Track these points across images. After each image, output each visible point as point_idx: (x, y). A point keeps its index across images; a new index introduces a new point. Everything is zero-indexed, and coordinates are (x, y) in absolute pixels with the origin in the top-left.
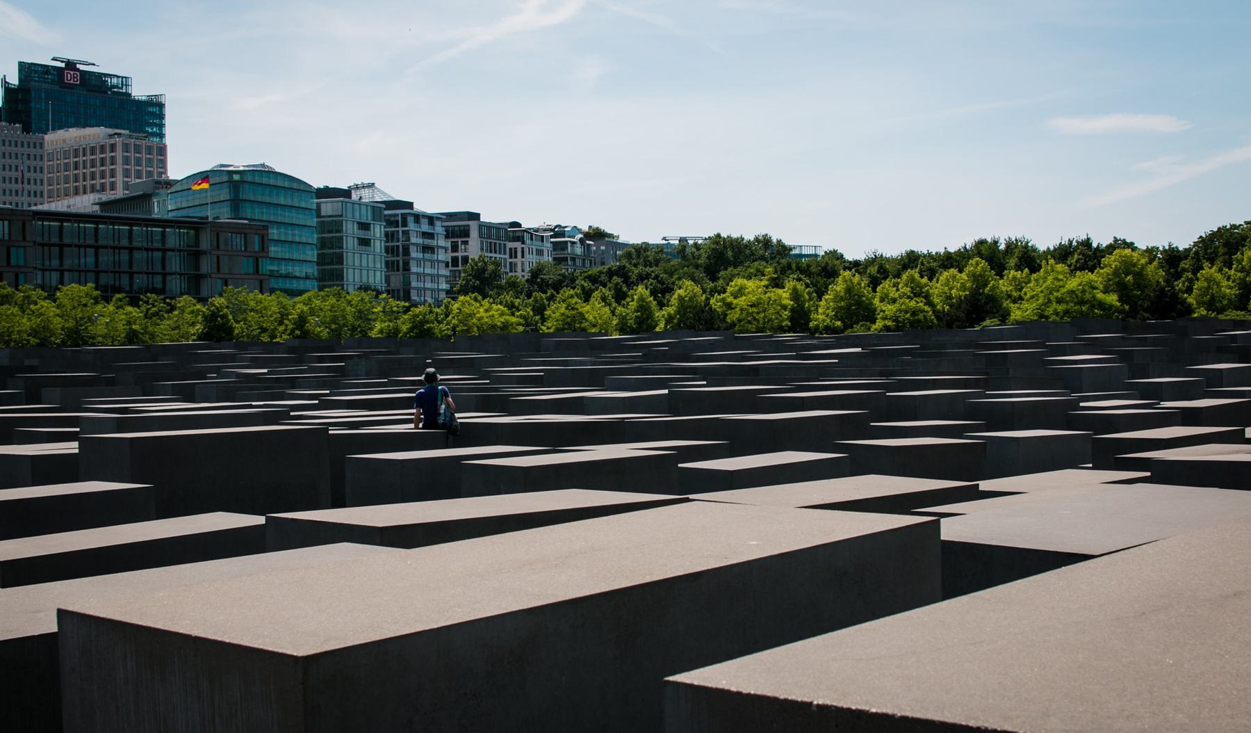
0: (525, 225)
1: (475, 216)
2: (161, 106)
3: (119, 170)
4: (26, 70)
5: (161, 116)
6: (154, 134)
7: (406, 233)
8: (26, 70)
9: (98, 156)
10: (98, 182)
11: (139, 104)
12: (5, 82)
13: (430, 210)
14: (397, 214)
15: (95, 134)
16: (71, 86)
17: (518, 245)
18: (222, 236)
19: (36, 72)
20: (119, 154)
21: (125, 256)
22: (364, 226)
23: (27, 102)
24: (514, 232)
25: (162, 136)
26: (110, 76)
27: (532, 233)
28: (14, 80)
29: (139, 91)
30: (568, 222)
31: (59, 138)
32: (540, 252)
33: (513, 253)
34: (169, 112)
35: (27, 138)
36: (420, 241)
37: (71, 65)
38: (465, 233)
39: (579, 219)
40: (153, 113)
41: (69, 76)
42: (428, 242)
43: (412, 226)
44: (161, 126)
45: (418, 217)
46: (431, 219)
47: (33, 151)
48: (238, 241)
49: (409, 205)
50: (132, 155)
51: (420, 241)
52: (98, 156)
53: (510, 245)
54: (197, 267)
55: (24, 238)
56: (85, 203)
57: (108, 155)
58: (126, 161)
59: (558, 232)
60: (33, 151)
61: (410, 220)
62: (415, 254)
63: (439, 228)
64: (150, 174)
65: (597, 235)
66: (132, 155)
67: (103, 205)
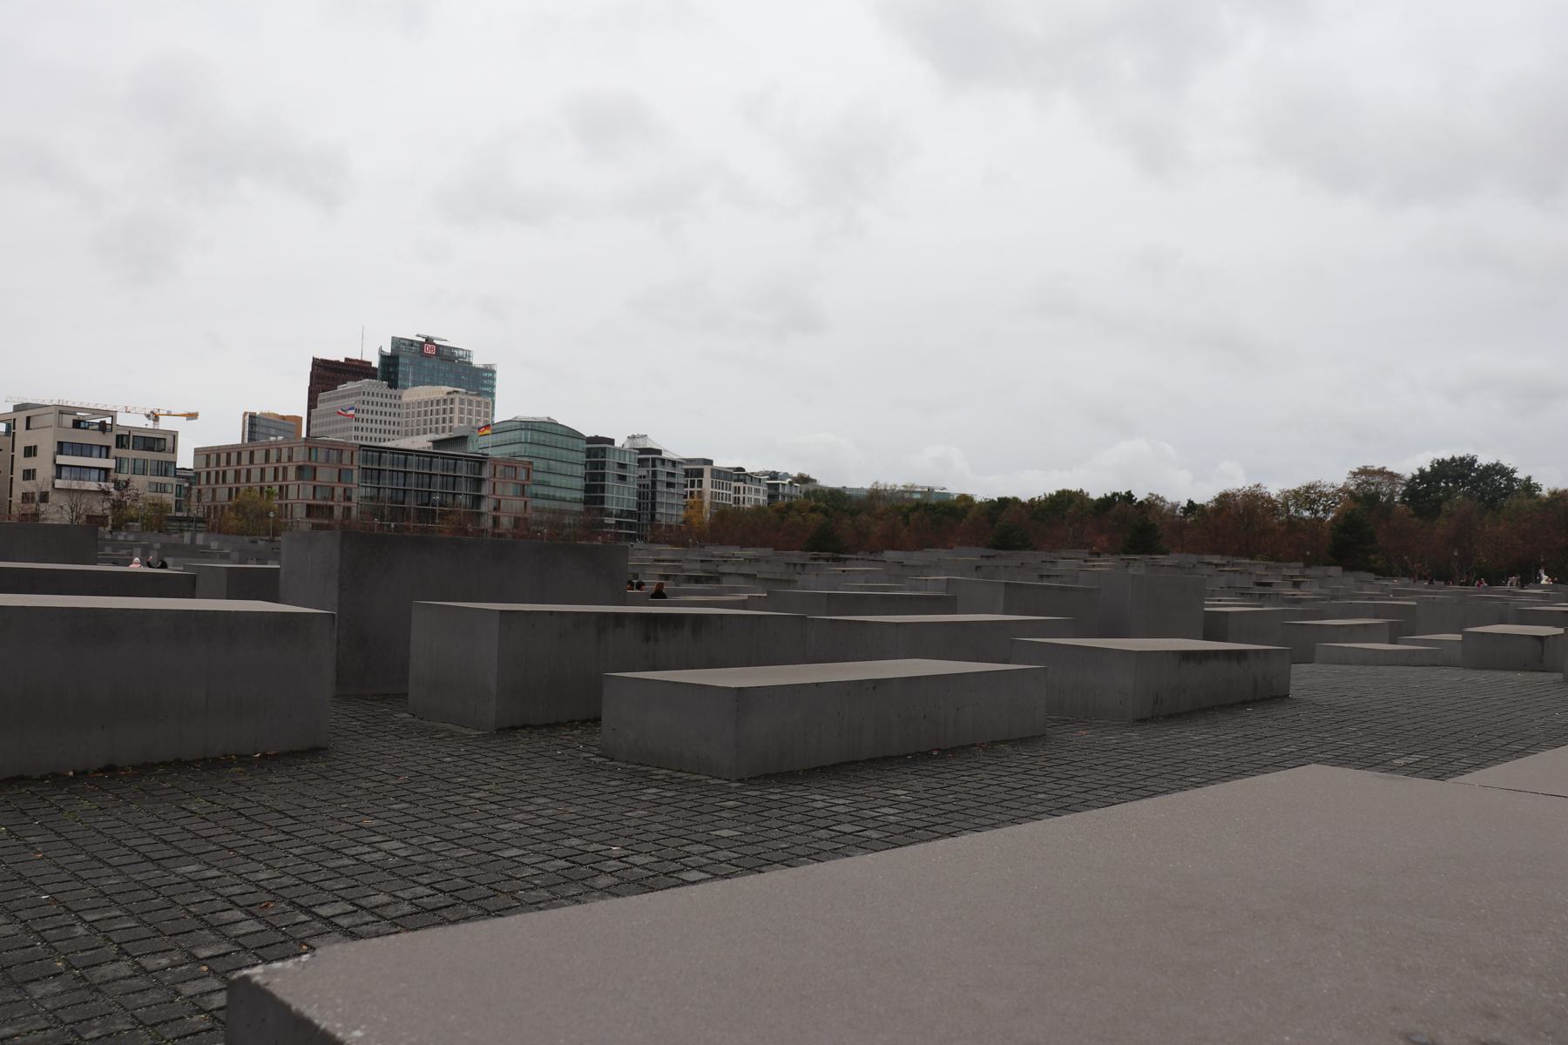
0: (748, 471)
1: (709, 462)
2: (494, 372)
3: (456, 416)
4: (397, 342)
5: (493, 379)
7: (654, 474)
8: (397, 342)
9: (442, 407)
10: (440, 425)
12: (381, 350)
13: (675, 457)
14: (649, 457)
15: (441, 391)
16: (429, 356)
17: (741, 484)
20: (457, 406)
21: (426, 479)
22: (623, 466)
23: (397, 365)
24: (739, 474)
25: (492, 394)
27: (751, 478)
29: (478, 361)
30: (780, 469)
31: (417, 394)
32: (757, 491)
33: (737, 490)
34: (498, 376)
35: (393, 392)
36: (665, 478)
37: (429, 340)
38: (700, 473)
39: (791, 468)
41: (428, 349)
42: (671, 480)
43: (659, 468)
44: (493, 386)
45: (663, 461)
46: (674, 463)
47: (394, 401)
48: (510, 472)
49: (659, 452)
50: (466, 407)
51: (665, 478)
52: (442, 407)
53: (734, 484)
54: (479, 490)
56: (422, 442)
57: (448, 407)
58: (461, 411)
59: (774, 476)
60: (394, 401)
61: (658, 463)
62: (661, 488)
63: (679, 471)
64: (470, 420)
65: (803, 479)
66: (466, 407)
67: (436, 443)
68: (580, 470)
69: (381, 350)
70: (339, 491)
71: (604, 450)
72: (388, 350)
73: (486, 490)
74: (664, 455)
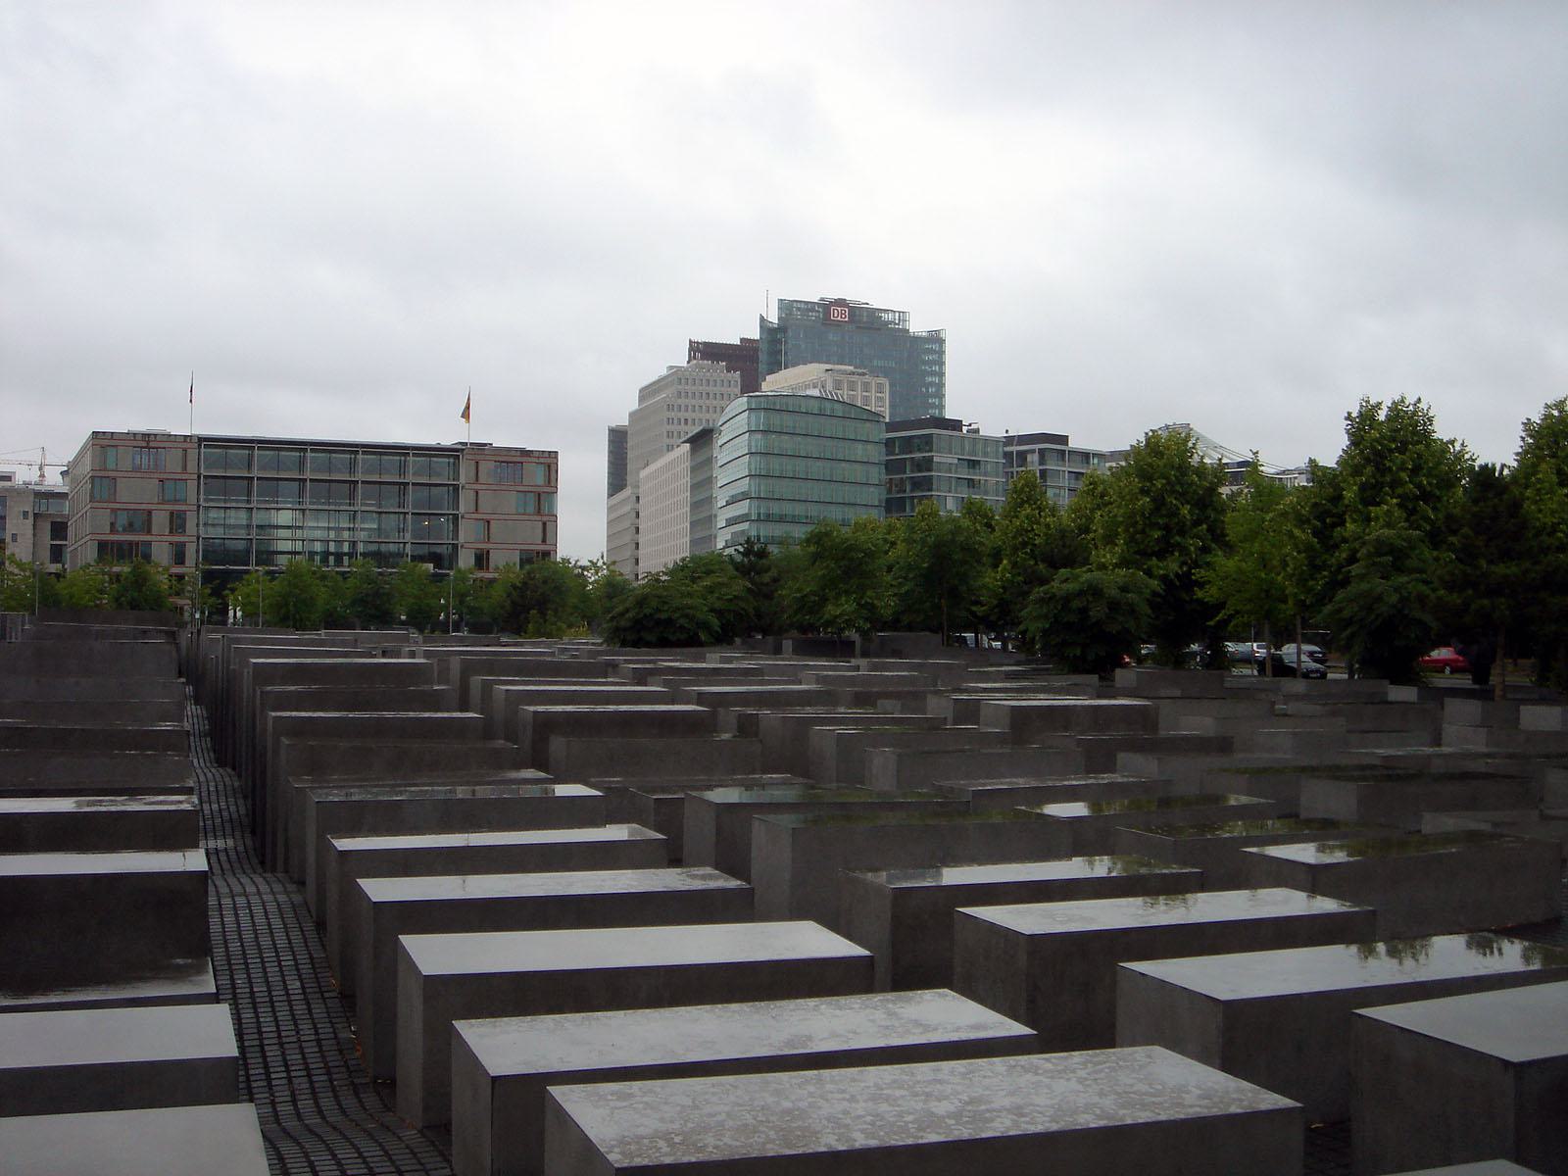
2: (942, 342)
4: (786, 307)
5: (942, 353)
6: (933, 374)
8: (786, 307)
11: (917, 340)
12: (762, 319)
16: (838, 324)
18: (483, 466)
19: (798, 309)
22: (973, 464)
26: (886, 311)
28: (773, 318)
29: (917, 326)
34: (948, 348)
40: (931, 351)
41: (836, 314)
44: (942, 364)
49: (1064, 440)
55: (185, 467)
68: (877, 475)
69: (762, 319)
70: (160, 520)
71: (928, 440)
72: (773, 318)
73: (465, 504)
74: (1073, 444)
